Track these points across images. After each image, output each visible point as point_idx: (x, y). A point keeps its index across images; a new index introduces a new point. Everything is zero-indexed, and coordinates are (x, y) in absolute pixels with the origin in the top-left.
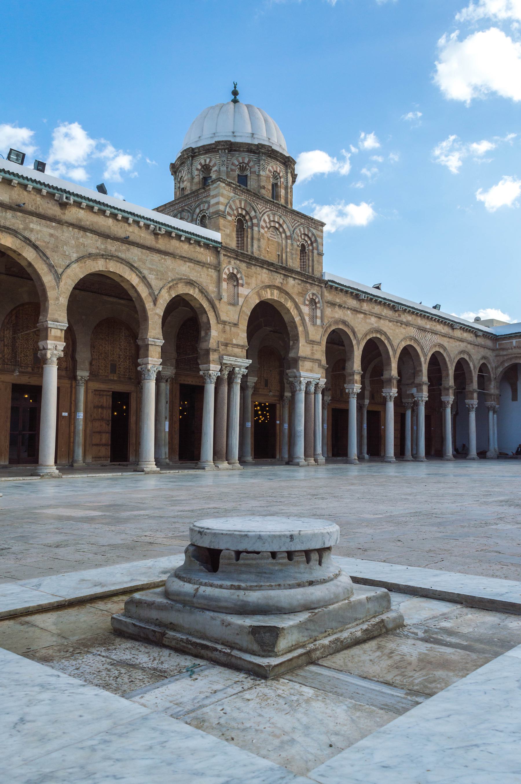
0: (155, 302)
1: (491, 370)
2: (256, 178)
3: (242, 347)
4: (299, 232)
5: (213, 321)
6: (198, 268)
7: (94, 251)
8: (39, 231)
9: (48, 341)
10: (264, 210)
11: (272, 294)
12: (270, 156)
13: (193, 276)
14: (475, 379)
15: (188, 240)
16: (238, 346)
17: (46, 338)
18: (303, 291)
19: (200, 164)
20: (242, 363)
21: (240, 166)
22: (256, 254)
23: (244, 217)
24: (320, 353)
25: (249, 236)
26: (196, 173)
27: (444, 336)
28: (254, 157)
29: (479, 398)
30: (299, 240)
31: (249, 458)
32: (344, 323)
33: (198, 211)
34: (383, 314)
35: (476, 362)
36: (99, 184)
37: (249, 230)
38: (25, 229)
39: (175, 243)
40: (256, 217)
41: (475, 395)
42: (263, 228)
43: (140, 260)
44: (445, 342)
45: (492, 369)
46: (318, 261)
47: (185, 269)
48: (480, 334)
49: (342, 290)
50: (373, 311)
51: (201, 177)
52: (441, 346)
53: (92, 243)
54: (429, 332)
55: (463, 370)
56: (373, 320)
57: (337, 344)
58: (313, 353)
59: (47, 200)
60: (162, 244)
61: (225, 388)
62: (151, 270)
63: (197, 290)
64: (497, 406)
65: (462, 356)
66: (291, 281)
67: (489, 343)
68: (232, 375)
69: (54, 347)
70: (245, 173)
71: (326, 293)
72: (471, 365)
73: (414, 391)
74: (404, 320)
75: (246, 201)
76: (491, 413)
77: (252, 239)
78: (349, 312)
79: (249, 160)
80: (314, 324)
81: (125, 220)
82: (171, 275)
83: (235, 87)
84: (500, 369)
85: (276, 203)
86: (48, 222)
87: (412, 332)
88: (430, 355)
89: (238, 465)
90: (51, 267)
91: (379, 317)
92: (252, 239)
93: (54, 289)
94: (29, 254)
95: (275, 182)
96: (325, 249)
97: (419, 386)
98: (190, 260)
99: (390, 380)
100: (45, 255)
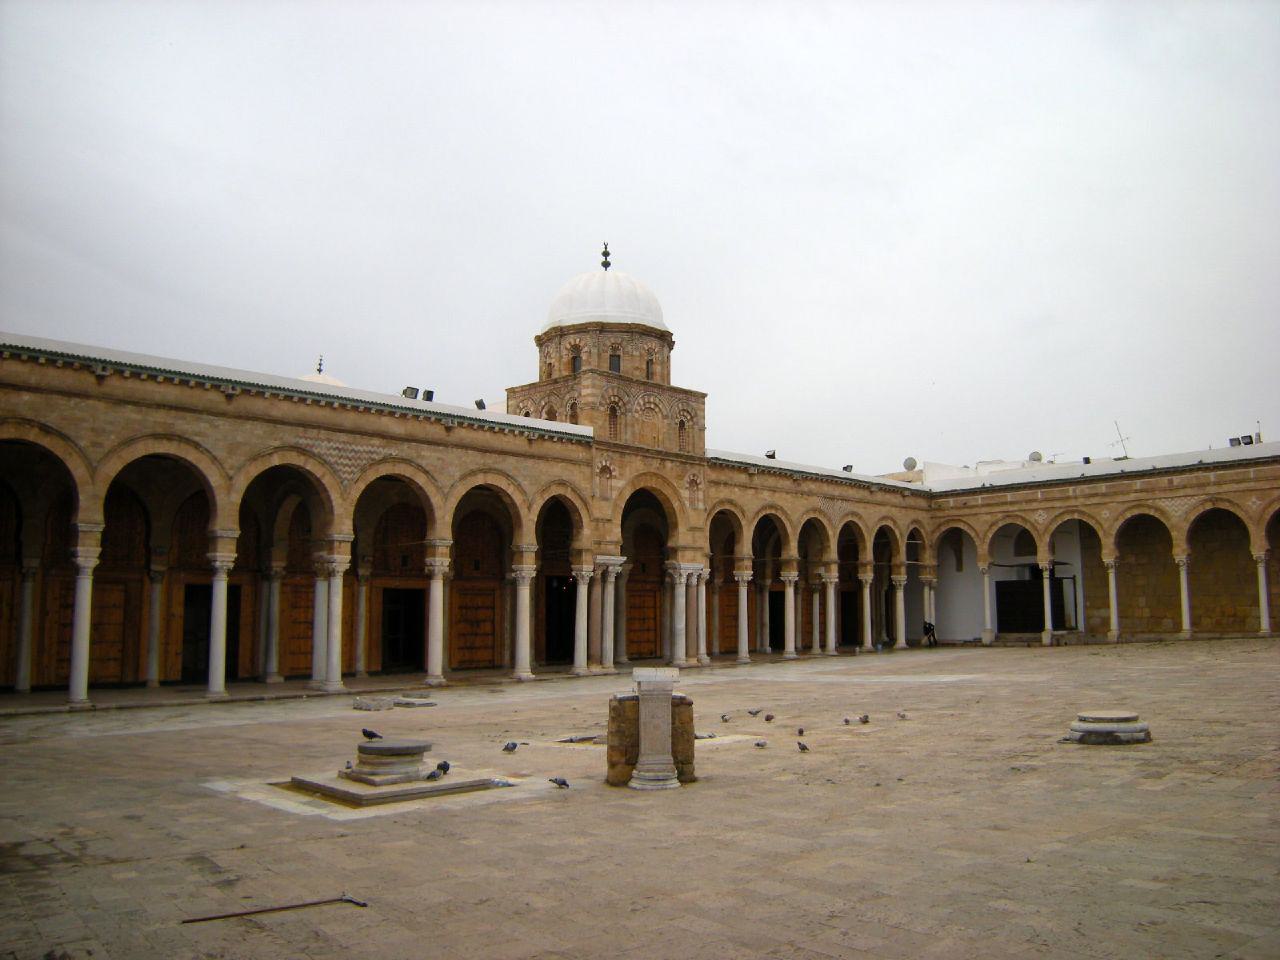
0: (529, 508)
1: (924, 535)
3: (617, 543)
5: (585, 520)
6: (571, 467)
7: (473, 467)
8: (429, 456)
9: (437, 559)
14: (903, 549)
15: (560, 440)
16: (611, 542)
17: (434, 555)
19: (570, 343)
20: (616, 561)
22: (629, 443)
23: (617, 403)
24: (703, 541)
26: (565, 352)
27: (860, 501)
28: (625, 336)
29: (908, 574)
31: (624, 659)
32: (731, 502)
33: (568, 397)
34: (779, 486)
35: (904, 529)
36: (478, 399)
38: (418, 457)
39: (548, 445)
41: (903, 570)
44: (859, 509)
45: (927, 534)
47: (558, 470)
48: (907, 493)
49: (727, 466)
50: (766, 484)
51: (571, 356)
52: (854, 514)
53: (473, 460)
55: (888, 538)
56: (766, 494)
57: (723, 527)
58: (694, 541)
59: (435, 426)
60: (536, 448)
61: (597, 589)
62: (525, 476)
63: (569, 489)
64: (935, 580)
65: (884, 523)
66: (669, 464)
67: (923, 503)
68: (605, 574)
69: (441, 562)
70: (618, 353)
71: (709, 471)
72: (897, 533)
73: (822, 571)
74: (806, 489)
76: (926, 590)
77: (626, 426)
78: (736, 489)
80: (695, 509)
81: (502, 431)
82: (544, 479)
84: (937, 534)
86: (437, 448)
87: (817, 502)
88: (840, 527)
89: (613, 670)
90: (439, 489)
91: (773, 490)
92: (626, 426)
93: (440, 508)
94: (421, 479)
96: (708, 423)
97: (827, 565)
98: (563, 460)
99: (788, 562)
100: (432, 477)
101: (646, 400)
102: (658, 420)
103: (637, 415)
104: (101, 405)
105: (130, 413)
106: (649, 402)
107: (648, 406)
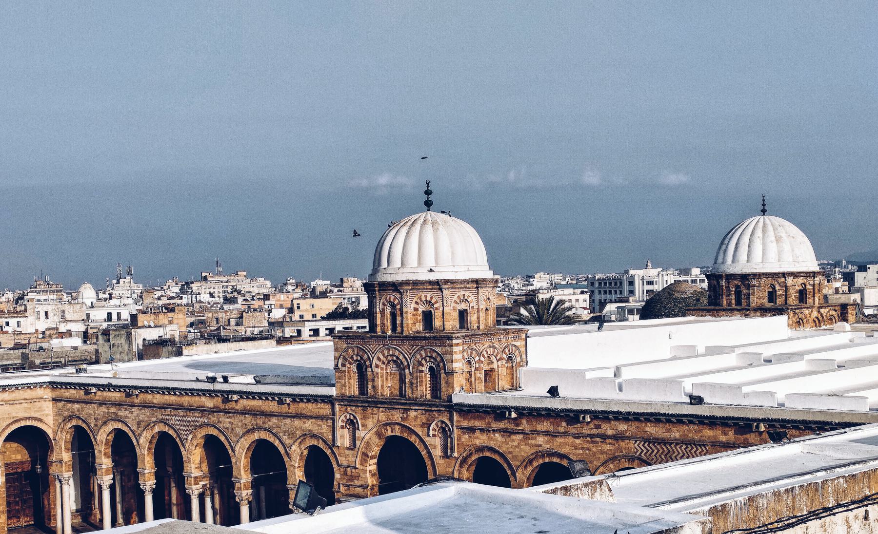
4: (418, 357)
5: (335, 466)
6: (319, 422)
11: (392, 431)
13: (315, 430)
18: (428, 420)
43: (277, 426)
46: (447, 382)
47: (309, 425)
50: (539, 428)
53: (249, 421)
54: (677, 444)
56: (541, 440)
62: (284, 432)
66: (412, 414)
74: (610, 432)
78: (497, 435)
82: (298, 433)
83: (428, 186)
91: (553, 435)
101: (386, 354)
104: (96, 406)
105: (104, 409)
107: (390, 358)
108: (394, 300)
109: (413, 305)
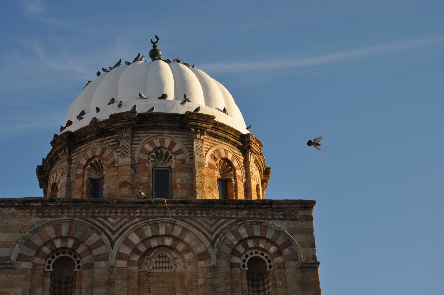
2: (115, 173)
4: (232, 237)
10: (125, 223)
12: (142, 128)
21: (91, 164)
25: (85, 282)
28: (109, 140)
30: (235, 253)
37: (84, 272)
40: (100, 243)
42: (120, 256)
75: (72, 221)
79: (103, 148)
83: (154, 46)
85: (156, 202)
92: (92, 286)
95: (168, 165)
102: (183, 265)
103: (122, 264)
106: (156, 236)
107: (154, 243)
108: (173, 144)
109: (208, 160)
